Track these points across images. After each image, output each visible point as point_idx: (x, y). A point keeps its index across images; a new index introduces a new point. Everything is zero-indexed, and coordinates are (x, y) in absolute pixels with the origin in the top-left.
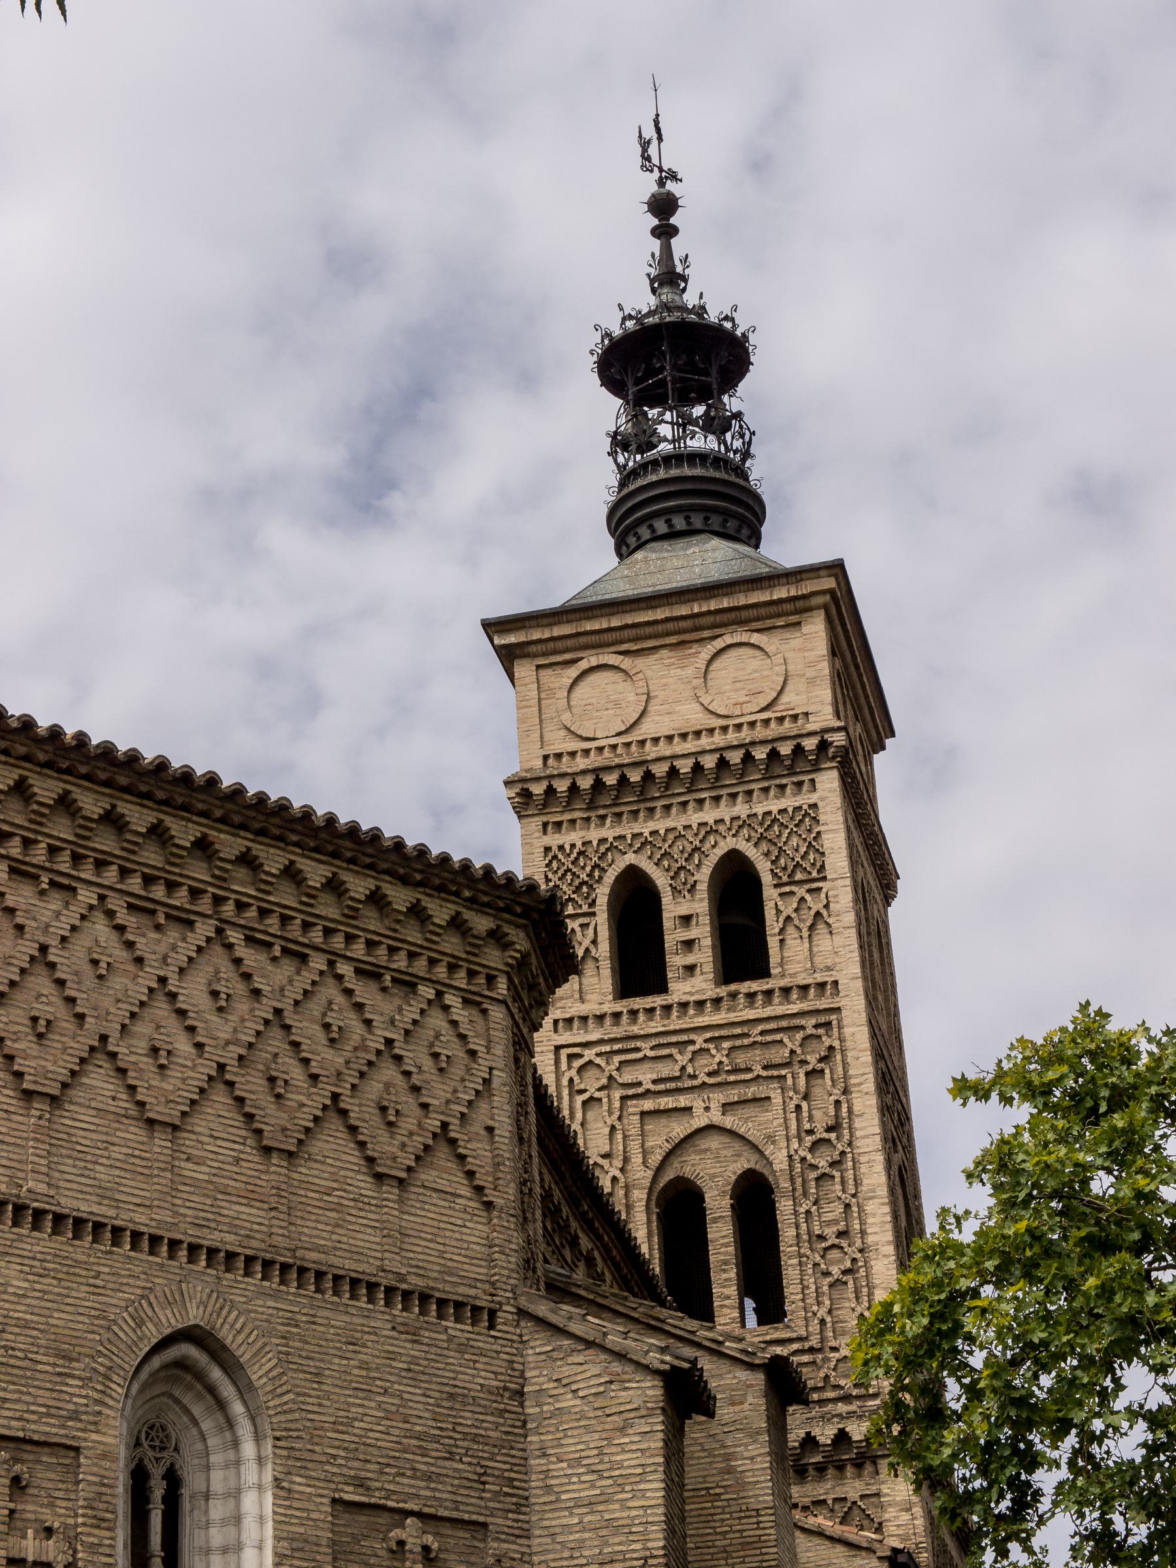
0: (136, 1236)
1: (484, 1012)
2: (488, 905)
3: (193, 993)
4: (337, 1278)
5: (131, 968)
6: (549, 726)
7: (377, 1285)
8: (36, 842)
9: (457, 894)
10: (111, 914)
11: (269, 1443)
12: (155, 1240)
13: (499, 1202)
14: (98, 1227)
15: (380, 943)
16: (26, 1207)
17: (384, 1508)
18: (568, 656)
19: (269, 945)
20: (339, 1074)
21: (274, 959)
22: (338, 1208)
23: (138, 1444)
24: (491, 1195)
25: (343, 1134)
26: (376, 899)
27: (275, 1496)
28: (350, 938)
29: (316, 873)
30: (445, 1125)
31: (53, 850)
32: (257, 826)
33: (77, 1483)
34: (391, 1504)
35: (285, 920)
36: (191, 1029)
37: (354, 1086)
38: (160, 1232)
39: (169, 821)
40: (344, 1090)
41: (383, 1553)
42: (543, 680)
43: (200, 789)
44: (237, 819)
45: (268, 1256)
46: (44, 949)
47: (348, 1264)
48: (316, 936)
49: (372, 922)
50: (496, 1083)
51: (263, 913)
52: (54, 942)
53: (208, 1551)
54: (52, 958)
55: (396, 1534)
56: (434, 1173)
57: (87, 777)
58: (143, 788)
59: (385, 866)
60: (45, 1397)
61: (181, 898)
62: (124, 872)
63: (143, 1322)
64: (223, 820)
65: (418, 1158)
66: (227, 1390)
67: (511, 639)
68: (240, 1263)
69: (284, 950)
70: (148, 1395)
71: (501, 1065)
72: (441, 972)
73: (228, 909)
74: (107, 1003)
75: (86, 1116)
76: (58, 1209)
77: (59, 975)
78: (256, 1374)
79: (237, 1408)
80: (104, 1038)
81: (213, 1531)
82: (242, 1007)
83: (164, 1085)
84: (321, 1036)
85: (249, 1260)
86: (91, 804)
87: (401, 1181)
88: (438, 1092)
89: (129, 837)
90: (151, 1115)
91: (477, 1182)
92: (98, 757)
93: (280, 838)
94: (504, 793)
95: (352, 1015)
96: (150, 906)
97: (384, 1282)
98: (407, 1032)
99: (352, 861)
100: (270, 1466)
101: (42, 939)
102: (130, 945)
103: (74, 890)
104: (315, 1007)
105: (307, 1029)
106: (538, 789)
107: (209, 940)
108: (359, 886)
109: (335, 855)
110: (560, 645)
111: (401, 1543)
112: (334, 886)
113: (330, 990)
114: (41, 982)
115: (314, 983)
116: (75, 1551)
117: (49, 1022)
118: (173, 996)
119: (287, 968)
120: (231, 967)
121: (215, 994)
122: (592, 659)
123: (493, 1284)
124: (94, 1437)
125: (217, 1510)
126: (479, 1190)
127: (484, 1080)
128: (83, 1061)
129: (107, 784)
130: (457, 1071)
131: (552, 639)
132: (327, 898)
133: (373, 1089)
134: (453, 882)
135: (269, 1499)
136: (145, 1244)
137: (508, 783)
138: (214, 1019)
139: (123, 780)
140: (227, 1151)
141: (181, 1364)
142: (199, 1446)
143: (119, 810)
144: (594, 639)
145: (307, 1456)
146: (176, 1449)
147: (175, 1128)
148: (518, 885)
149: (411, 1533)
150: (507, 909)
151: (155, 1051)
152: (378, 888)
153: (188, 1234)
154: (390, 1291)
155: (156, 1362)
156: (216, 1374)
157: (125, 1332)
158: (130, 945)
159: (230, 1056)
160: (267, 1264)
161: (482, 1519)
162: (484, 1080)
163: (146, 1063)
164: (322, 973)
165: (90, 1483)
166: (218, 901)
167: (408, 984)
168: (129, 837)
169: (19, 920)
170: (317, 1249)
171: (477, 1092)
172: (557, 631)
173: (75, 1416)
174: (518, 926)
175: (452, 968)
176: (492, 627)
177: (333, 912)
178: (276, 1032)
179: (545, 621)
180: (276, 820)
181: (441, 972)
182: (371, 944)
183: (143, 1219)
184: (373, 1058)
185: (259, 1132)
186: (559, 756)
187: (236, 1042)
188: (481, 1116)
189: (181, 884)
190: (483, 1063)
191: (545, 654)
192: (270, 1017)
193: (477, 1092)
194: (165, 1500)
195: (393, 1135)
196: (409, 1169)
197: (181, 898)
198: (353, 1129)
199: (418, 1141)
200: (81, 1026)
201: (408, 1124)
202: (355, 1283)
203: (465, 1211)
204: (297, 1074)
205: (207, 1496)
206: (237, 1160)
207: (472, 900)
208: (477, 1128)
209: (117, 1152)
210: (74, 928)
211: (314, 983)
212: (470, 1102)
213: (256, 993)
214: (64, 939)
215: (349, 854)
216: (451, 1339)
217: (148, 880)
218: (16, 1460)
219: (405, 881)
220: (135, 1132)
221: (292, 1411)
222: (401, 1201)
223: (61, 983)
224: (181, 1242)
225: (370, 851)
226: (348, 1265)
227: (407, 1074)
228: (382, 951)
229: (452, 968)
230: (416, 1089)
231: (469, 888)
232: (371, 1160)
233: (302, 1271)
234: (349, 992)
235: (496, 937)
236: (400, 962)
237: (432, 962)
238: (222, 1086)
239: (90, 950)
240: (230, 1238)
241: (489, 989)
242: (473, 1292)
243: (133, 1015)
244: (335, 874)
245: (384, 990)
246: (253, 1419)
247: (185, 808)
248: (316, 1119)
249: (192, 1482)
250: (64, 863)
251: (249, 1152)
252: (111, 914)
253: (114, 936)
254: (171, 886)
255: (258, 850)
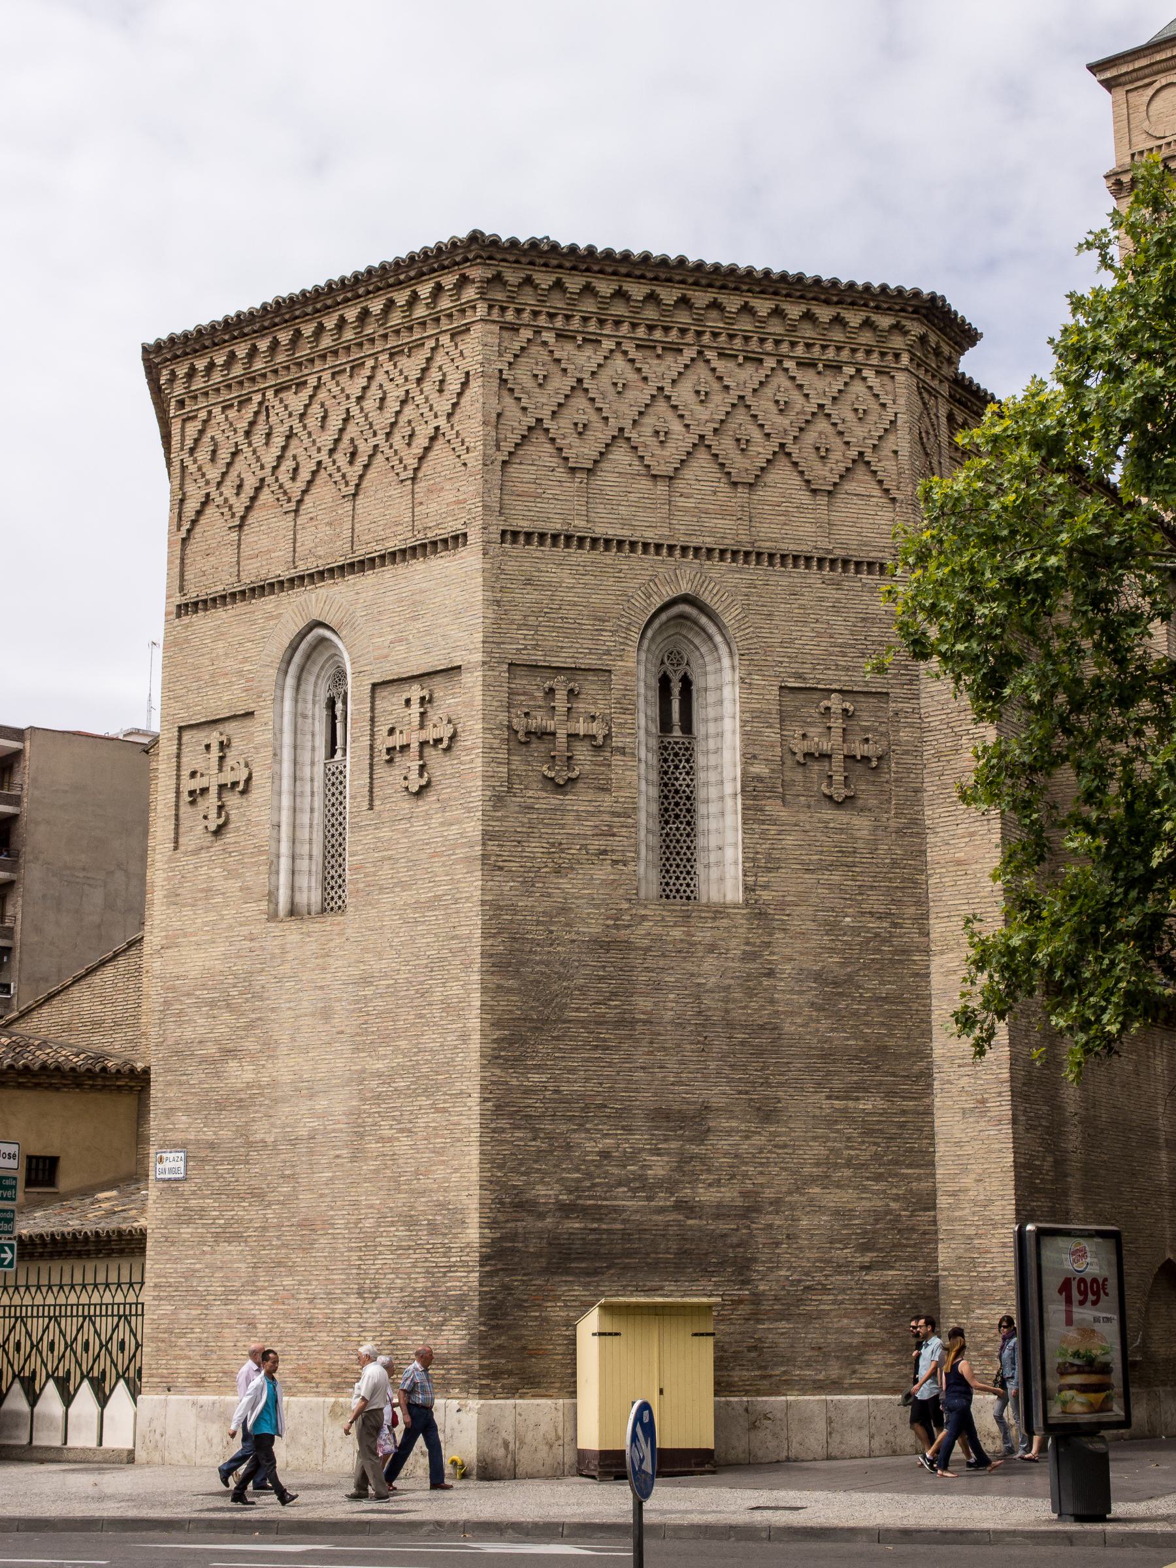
0: (646, 546)
1: (893, 377)
2: (889, 309)
3: (684, 393)
4: (783, 557)
5: (640, 384)
6: (1135, 133)
7: (812, 558)
8: (573, 316)
9: (866, 305)
10: (625, 353)
11: (737, 658)
12: (658, 547)
13: (899, 497)
14: (620, 543)
15: (814, 344)
16: (573, 536)
17: (816, 689)
18: (1147, 81)
19: (736, 356)
20: (785, 431)
21: (740, 365)
22: (786, 513)
23: (662, 663)
24: (894, 493)
25: (789, 467)
26: (808, 316)
27: (741, 688)
28: (793, 344)
29: (763, 306)
30: (861, 454)
31: (585, 320)
32: (718, 284)
33: (611, 690)
34: (820, 686)
35: (747, 339)
36: (681, 416)
37: (795, 438)
38: (661, 542)
39: (658, 290)
40: (789, 441)
41: (817, 715)
42: (1131, 100)
43: (674, 268)
44: (704, 282)
45: (735, 548)
46: (580, 381)
47: (791, 547)
48: (769, 346)
49: (807, 331)
50: (899, 422)
51: (731, 337)
52: (586, 376)
53: (707, 721)
54: (585, 386)
55: (825, 703)
56: (854, 484)
57: (601, 272)
58: (638, 273)
59: (811, 295)
60: (588, 644)
61: (673, 336)
62: (634, 326)
63: (651, 595)
64: (696, 284)
65: (841, 477)
66: (712, 629)
67: (1108, 75)
68: (716, 554)
69: (745, 358)
70: (665, 635)
71: (903, 411)
72: (860, 356)
73: (706, 338)
74: (623, 408)
75: (611, 477)
76: (594, 535)
77: (591, 395)
78: (727, 619)
79: (718, 639)
80: (621, 430)
81: (709, 709)
82: (717, 398)
83: (664, 453)
84: (774, 409)
85: (723, 552)
86: (605, 288)
87: (830, 492)
88: (858, 433)
89: (632, 304)
90: (653, 472)
91: (885, 487)
92: (604, 259)
93: (736, 289)
94: (1104, 183)
95: (796, 392)
96: (652, 344)
97: (817, 555)
98: (834, 398)
99: (787, 296)
100: (737, 671)
101: (578, 375)
102: (639, 370)
103: (600, 341)
104: (769, 391)
105: (764, 406)
106: (1126, 179)
107: (693, 360)
108: (794, 311)
109: (776, 293)
110: (1140, 73)
111: (828, 709)
112: (777, 312)
113: (781, 380)
114: (580, 402)
115: (767, 376)
116: (610, 728)
117: (585, 425)
118: (668, 398)
119: (750, 368)
120: (709, 373)
121: (698, 392)
122: (1162, 80)
123: (895, 548)
124: (620, 663)
125: (711, 697)
126: (887, 491)
127: (891, 422)
128: (607, 445)
129: (615, 273)
130: (872, 418)
131: (1134, 71)
132: (774, 320)
133: (810, 437)
134: (862, 298)
135: (737, 689)
136: (652, 550)
137: (1106, 177)
138: (698, 408)
139: (623, 270)
140: (706, 488)
141: (682, 616)
142: (701, 661)
143: (624, 288)
144: (1163, 65)
145: (762, 663)
146: (688, 664)
147: (671, 478)
148: (906, 294)
149: (835, 703)
150: (902, 310)
151: (657, 433)
152: (809, 310)
153: (682, 540)
154: (821, 561)
155: (664, 617)
156: (704, 620)
157: (639, 601)
158: (639, 370)
159: (707, 430)
160: (735, 553)
161: (885, 690)
162: (891, 422)
163: (652, 441)
164: (773, 369)
165: (619, 690)
166: (699, 334)
167: (836, 367)
168: (632, 304)
169: (563, 366)
170: (770, 540)
171: (886, 430)
172: (1138, 65)
173: (608, 652)
174: (913, 319)
175: (868, 352)
176: (1094, 68)
177: (779, 329)
178: (741, 410)
179: (1129, 58)
180: (732, 279)
181: (860, 356)
182: (808, 346)
183: (651, 535)
184: (809, 418)
185: (729, 473)
186: (1141, 153)
187: (712, 421)
188: (890, 443)
189: (673, 327)
190: (890, 411)
191: (1131, 82)
192: (736, 402)
193: (886, 430)
194: (681, 693)
195: (824, 464)
196: (835, 484)
197: (673, 336)
198: (795, 464)
199: (841, 467)
200: (607, 425)
201: (836, 455)
202: (796, 558)
203: (877, 505)
204: (757, 435)
205: (706, 690)
206: (715, 493)
207: (877, 307)
208: (886, 451)
209: (632, 497)
210: (600, 366)
211: (767, 376)
212: (880, 437)
213: (727, 388)
214: (593, 373)
215: (784, 292)
216: (864, 585)
217: (651, 328)
218: (570, 680)
219: (827, 302)
220: (645, 484)
221: (751, 638)
222: (829, 504)
223: (592, 400)
224: (675, 546)
225: (799, 287)
226: (792, 547)
227: (835, 425)
228: (817, 349)
229: (868, 352)
230: (841, 433)
231: (873, 300)
232: (808, 482)
233: (759, 555)
234: (793, 378)
235: (897, 327)
236: (831, 354)
237: (854, 351)
238: (703, 449)
239: (612, 377)
240: (708, 540)
241: (897, 363)
242: (880, 555)
243: (641, 413)
244: (777, 306)
245: (819, 373)
246: (728, 644)
247: (669, 280)
248: (768, 461)
249: (698, 682)
250: (592, 327)
251: (723, 487)
252: (625, 353)
253: (629, 366)
254: (667, 329)
255: (722, 298)
